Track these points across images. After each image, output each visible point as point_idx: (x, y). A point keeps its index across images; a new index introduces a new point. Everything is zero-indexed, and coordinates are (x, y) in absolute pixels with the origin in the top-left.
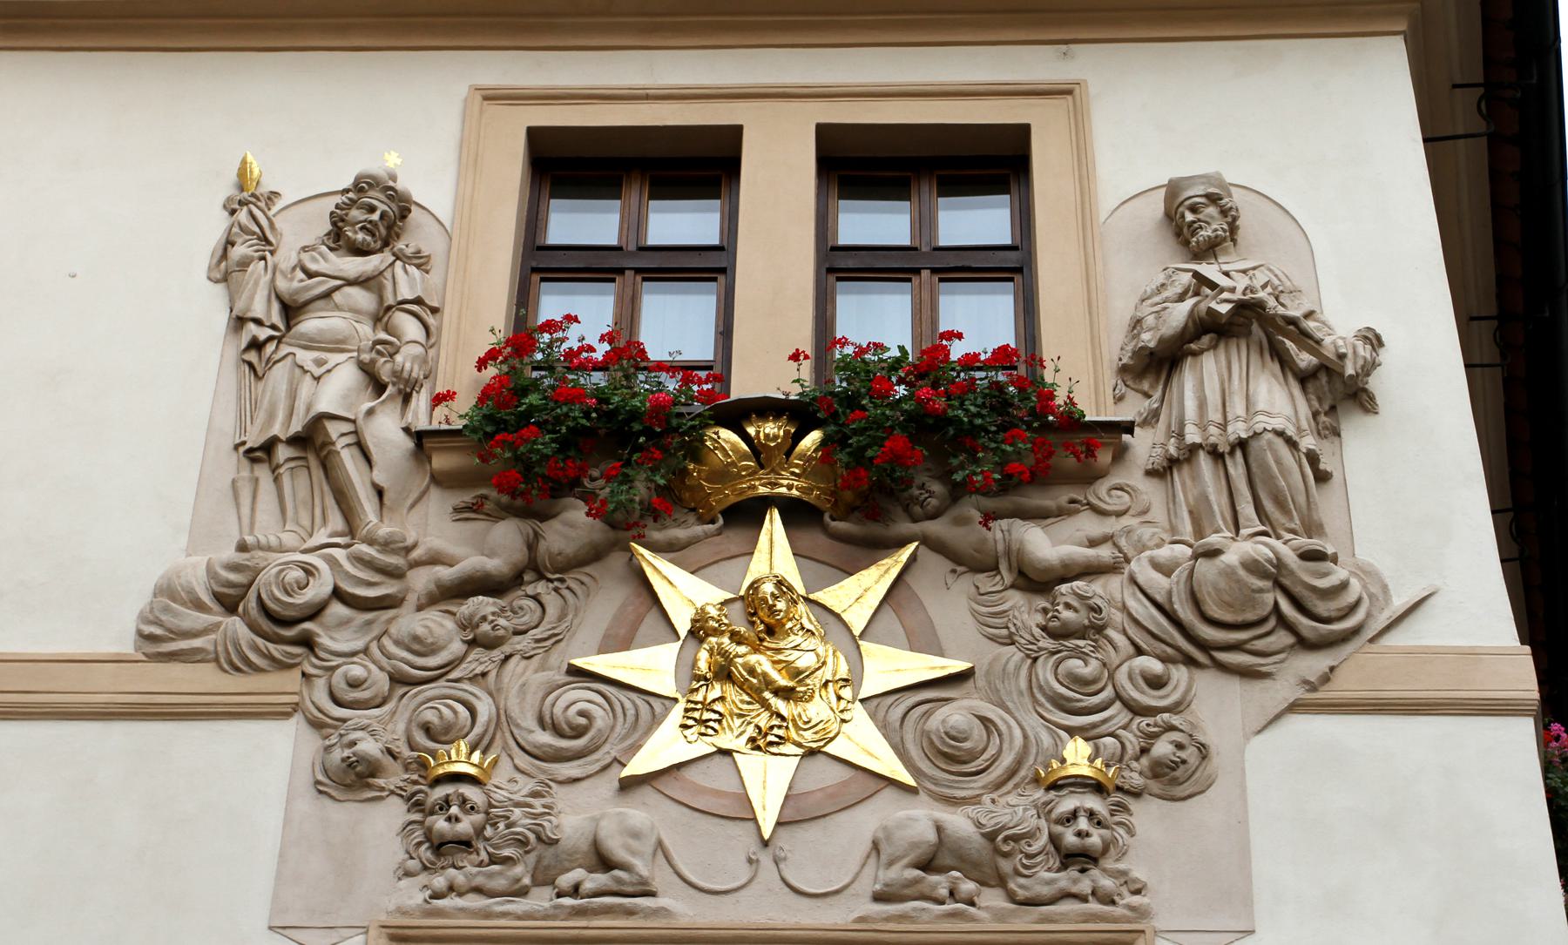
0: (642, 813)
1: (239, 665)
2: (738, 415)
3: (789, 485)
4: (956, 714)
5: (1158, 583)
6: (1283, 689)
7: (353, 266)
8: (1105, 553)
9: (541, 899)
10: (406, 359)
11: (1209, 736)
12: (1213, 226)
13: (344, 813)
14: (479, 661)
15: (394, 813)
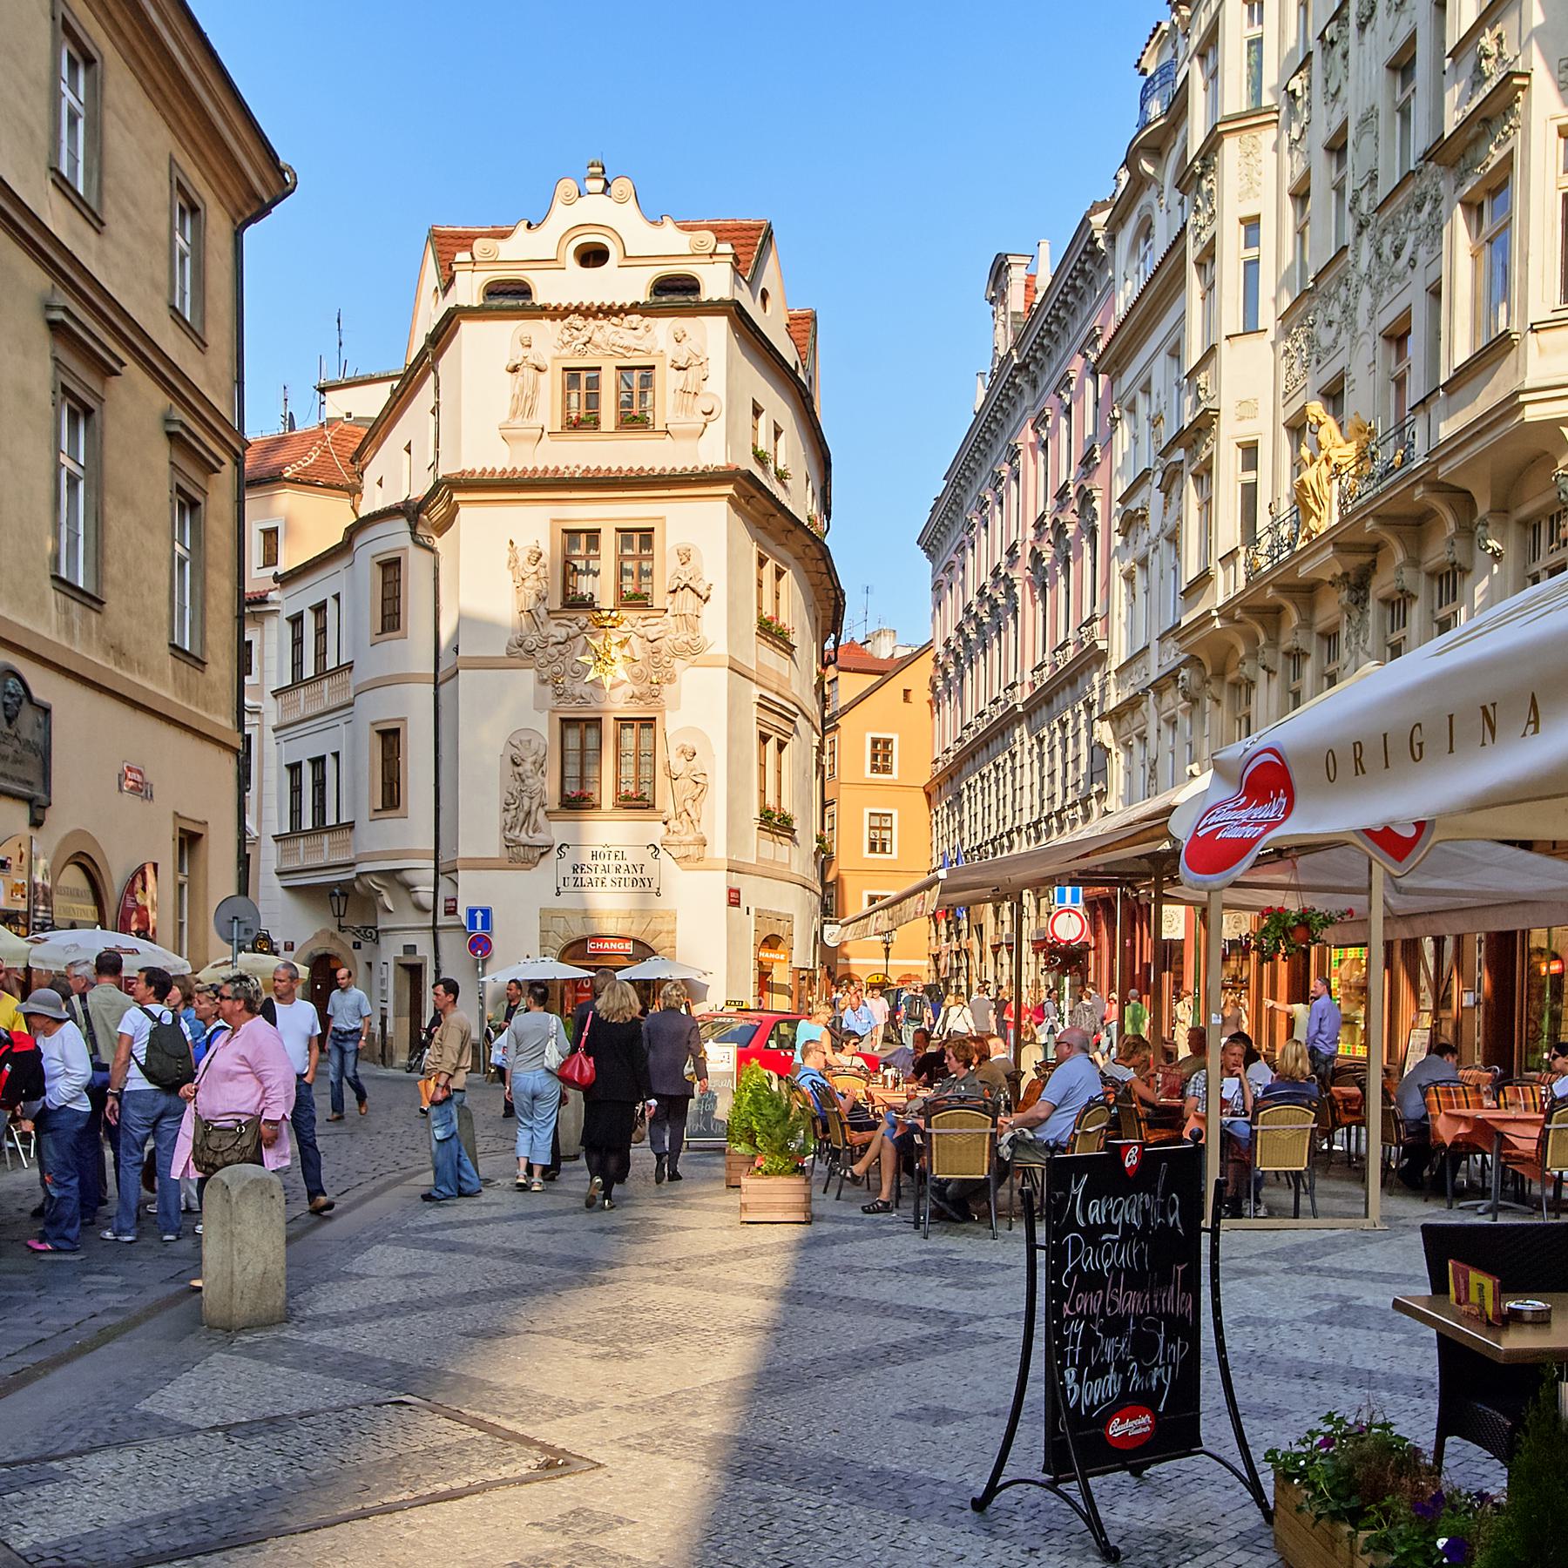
0: (588, 689)
1: (522, 658)
2: (599, 611)
3: (609, 623)
4: (636, 670)
5: (670, 644)
6: (688, 663)
7: (534, 569)
8: (661, 635)
9: (574, 704)
10: (544, 594)
11: (677, 673)
12: (685, 560)
13: (543, 687)
14: (562, 658)
15: (550, 688)
